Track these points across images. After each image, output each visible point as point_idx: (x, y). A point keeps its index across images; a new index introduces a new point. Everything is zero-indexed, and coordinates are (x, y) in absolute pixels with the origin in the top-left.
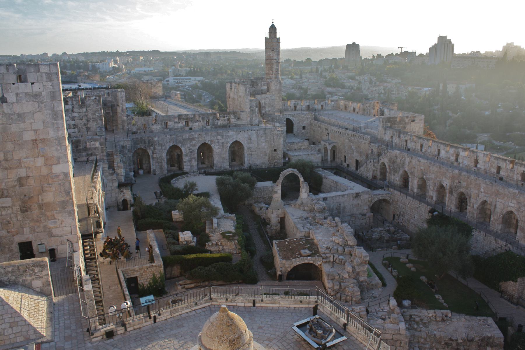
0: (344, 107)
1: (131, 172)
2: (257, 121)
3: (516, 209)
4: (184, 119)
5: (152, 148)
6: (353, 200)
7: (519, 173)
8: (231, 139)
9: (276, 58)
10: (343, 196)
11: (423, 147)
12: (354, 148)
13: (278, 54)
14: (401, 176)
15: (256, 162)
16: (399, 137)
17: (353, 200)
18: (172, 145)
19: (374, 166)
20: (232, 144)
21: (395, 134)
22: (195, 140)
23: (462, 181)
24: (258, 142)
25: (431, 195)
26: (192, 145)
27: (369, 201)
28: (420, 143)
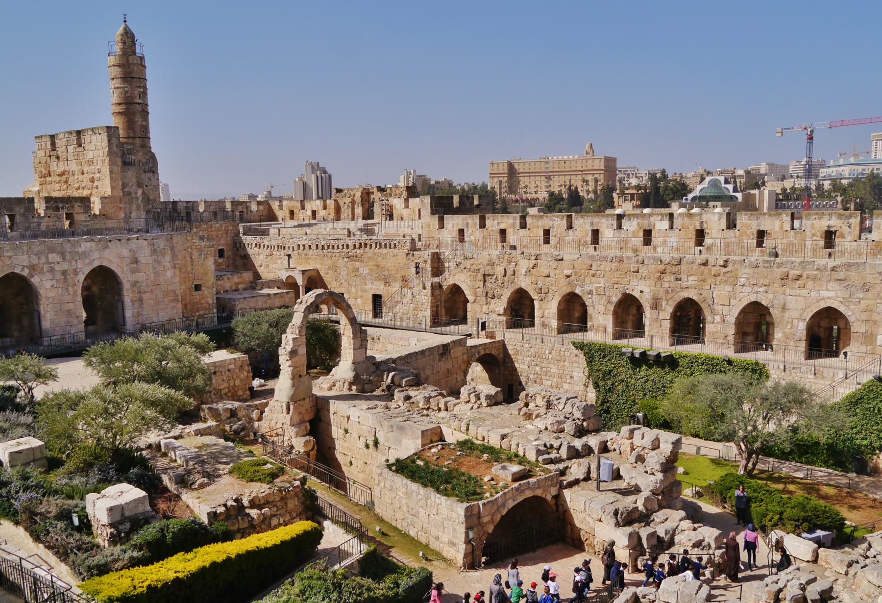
0: (288, 215)
3: (840, 299)
6: (439, 360)
7: (818, 234)
8: (87, 261)
9: (139, 101)
10: (422, 352)
11: (552, 234)
12: (364, 270)
13: (144, 94)
14: (508, 303)
15: (155, 320)
16: (483, 225)
17: (439, 360)
19: (433, 294)
20: (85, 279)
21: (470, 222)
23: (684, 277)
25: (602, 322)
28: (542, 226)
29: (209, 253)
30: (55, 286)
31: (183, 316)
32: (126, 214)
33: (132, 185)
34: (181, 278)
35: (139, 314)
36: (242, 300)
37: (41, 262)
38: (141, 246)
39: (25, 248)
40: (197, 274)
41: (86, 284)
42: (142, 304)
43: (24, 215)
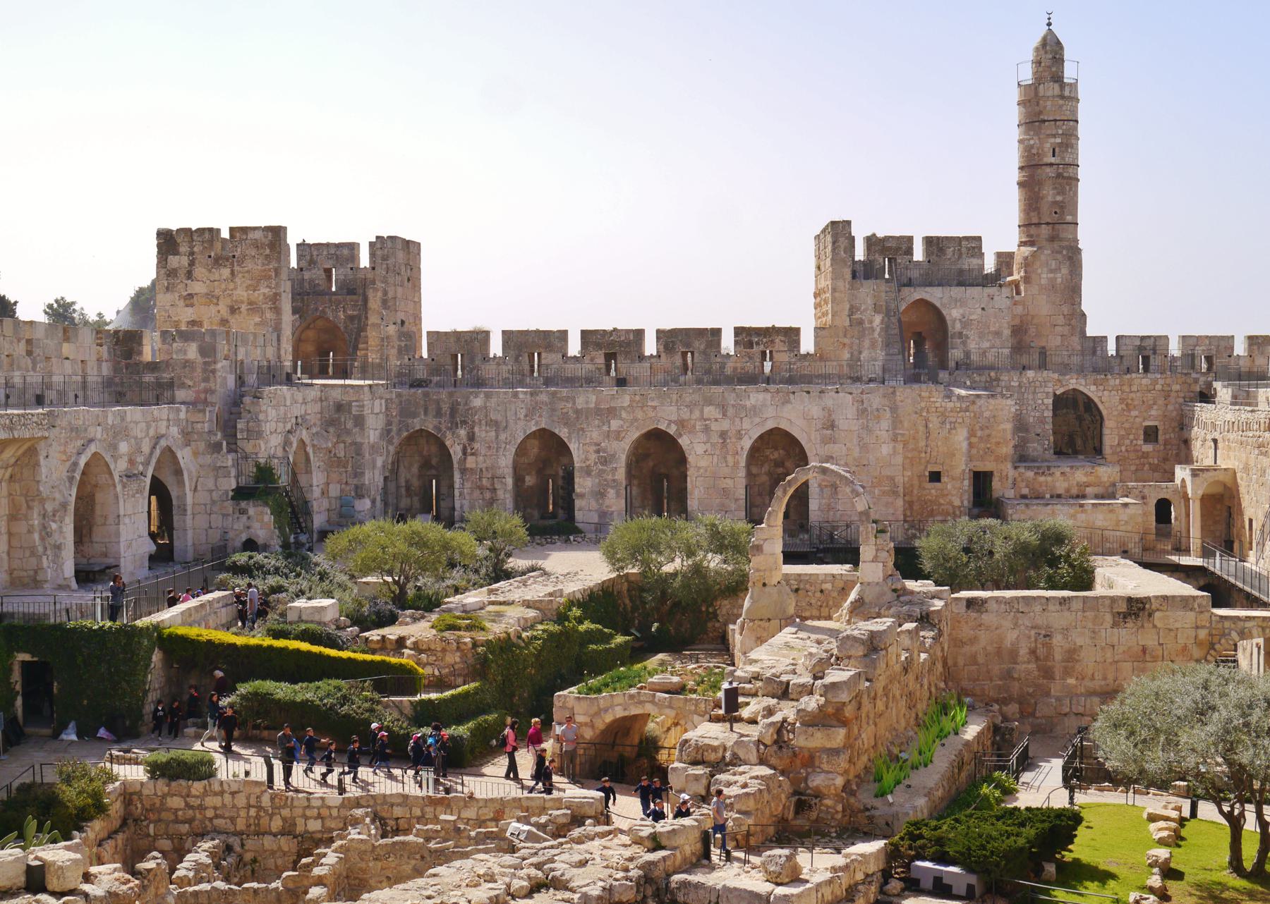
1: (361, 497)
2: (879, 364)
4: (598, 346)
5: (463, 432)
6: (1115, 625)
9: (1053, 160)
17: (1115, 625)
18: (534, 429)
22: (621, 419)
24: (860, 438)
26: (608, 435)
27: (1198, 643)
29: (960, 420)
30: (709, 452)
31: (905, 521)
32: (852, 354)
33: (866, 310)
34: (906, 458)
35: (830, 508)
36: (1023, 507)
37: (694, 417)
38: (843, 403)
39: (675, 397)
40: (934, 454)
41: (775, 455)
42: (836, 493)
43: (704, 353)
